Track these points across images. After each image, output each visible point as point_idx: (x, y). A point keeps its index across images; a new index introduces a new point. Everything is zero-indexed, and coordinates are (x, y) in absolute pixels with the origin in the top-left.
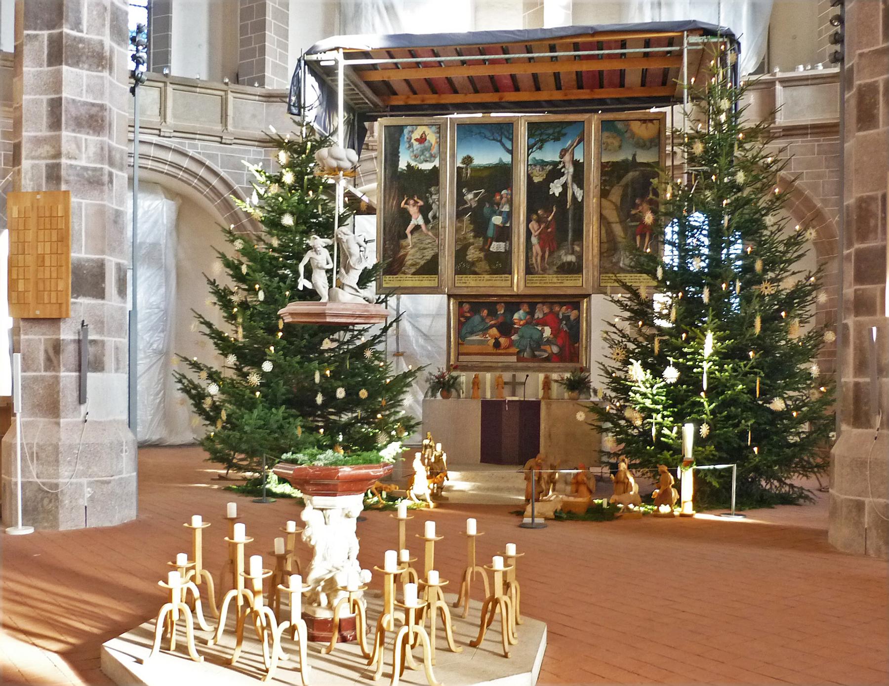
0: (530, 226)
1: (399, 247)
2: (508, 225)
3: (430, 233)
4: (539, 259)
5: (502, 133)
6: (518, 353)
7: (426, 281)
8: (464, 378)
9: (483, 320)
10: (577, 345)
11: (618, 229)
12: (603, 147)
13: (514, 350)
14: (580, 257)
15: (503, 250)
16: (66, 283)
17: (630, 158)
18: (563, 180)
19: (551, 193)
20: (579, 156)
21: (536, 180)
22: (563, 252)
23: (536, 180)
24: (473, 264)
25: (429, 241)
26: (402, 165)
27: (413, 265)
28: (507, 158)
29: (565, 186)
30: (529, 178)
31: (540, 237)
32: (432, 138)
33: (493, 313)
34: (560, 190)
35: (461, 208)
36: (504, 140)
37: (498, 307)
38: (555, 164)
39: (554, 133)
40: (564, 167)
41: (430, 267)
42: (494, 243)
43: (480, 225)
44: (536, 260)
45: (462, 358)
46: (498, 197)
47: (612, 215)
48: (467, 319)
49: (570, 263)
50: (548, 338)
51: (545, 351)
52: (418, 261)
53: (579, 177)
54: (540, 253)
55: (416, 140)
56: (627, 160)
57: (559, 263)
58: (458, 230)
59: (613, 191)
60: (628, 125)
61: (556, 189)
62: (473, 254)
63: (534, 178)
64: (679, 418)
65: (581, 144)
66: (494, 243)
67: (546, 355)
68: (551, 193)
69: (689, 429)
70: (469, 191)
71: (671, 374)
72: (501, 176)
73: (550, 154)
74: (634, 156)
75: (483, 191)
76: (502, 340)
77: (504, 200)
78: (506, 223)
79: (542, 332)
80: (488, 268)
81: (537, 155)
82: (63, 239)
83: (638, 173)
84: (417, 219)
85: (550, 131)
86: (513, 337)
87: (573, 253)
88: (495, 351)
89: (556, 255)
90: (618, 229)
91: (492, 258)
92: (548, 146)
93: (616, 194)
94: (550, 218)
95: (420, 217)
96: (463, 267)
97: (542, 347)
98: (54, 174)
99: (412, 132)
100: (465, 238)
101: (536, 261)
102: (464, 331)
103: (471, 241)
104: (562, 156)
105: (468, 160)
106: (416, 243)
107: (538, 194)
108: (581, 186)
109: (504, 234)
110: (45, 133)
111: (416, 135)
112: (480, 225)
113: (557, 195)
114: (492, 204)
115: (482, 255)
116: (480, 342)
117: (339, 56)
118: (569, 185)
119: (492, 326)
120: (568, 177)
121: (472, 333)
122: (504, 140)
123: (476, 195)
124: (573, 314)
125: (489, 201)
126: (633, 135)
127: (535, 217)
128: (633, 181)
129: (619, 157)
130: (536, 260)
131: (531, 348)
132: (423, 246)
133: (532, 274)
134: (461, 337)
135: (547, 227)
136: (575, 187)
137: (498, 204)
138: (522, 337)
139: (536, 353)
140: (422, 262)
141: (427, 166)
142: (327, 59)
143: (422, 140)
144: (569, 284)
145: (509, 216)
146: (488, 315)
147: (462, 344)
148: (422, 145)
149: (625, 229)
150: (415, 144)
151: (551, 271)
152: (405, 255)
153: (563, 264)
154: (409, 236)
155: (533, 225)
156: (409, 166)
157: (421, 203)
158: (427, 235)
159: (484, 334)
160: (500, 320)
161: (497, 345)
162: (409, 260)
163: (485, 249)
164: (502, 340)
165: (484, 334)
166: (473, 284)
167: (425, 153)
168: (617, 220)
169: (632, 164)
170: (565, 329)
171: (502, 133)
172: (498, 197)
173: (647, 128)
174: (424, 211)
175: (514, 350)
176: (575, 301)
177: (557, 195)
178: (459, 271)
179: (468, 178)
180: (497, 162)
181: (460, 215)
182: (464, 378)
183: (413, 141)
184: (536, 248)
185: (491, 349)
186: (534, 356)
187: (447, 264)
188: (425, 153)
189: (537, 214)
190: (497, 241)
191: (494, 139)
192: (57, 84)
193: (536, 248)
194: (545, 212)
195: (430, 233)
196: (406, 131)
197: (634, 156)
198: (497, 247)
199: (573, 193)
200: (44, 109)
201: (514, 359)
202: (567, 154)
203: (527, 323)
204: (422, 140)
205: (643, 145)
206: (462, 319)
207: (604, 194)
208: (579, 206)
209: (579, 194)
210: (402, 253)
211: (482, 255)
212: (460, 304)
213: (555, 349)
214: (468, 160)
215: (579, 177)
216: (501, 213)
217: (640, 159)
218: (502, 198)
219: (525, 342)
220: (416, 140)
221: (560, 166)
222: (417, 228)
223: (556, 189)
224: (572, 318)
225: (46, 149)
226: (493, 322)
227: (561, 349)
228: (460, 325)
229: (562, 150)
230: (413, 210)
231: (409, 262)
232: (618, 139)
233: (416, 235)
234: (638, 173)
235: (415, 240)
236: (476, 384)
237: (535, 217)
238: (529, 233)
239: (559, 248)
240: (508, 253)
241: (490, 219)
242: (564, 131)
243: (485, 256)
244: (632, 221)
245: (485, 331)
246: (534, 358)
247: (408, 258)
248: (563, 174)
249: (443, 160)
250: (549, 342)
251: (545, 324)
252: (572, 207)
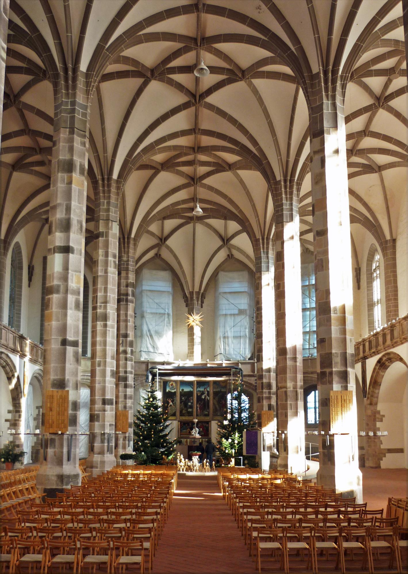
7: (173, 418)
8: (183, 440)
11: (217, 406)
12: (214, 388)
14: (209, 412)
16: (127, 426)
20: (208, 390)
26: (167, 391)
28: (192, 390)
29: (205, 396)
30: (197, 394)
32: (174, 384)
33: (188, 425)
41: (174, 415)
43: (186, 405)
47: (216, 403)
53: (208, 394)
58: (180, 406)
62: (184, 412)
64: (232, 449)
69: (233, 451)
71: (230, 440)
72: (190, 394)
73: (202, 389)
81: (199, 389)
82: (127, 418)
84: (171, 403)
90: (217, 406)
93: (217, 398)
96: (182, 414)
98: (125, 407)
101: (199, 413)
105: (183, 390)
107: (199, 398)
109: (191, 407)
110: (123, 400)
111: (171, 384)
112: (186, 405)
117: (157, 370)
120: (206, 394)
124: (207, 425)
129: (218, 390)
134: (181, 430)
141: (173, 391)
142: (155, 370)
143: (172, 385)
144: (207, 419)
145: (192, 403)
155: (198, 405)
163: (187, 410)
166: (184, 418)
167: (172, 388)
169: (221, 392)
174: (172, 401)
176: (208, 423)
179: (183, 394)
181: (181, 402)
182: (183, 440)
184: (199, 410)
187: (178, 414)
188: (172, 388)
192: (126, 392)
193: (199, 410)
198: (190, 410)
200: (123, 396)
204: (172, 385)
207: (214, 398)
208: (208, 401)
209: (208, 398)
212: (181, 423)
214: (183, 390)
215: (208, 394)
222: (171, 405)
223: (203, 397)
225: (124, 403)
228: (181, 427)
230: (170, 401)
236: (186, 442)
240: (192, 411)
245: (186, 429)
249: (177, 390)
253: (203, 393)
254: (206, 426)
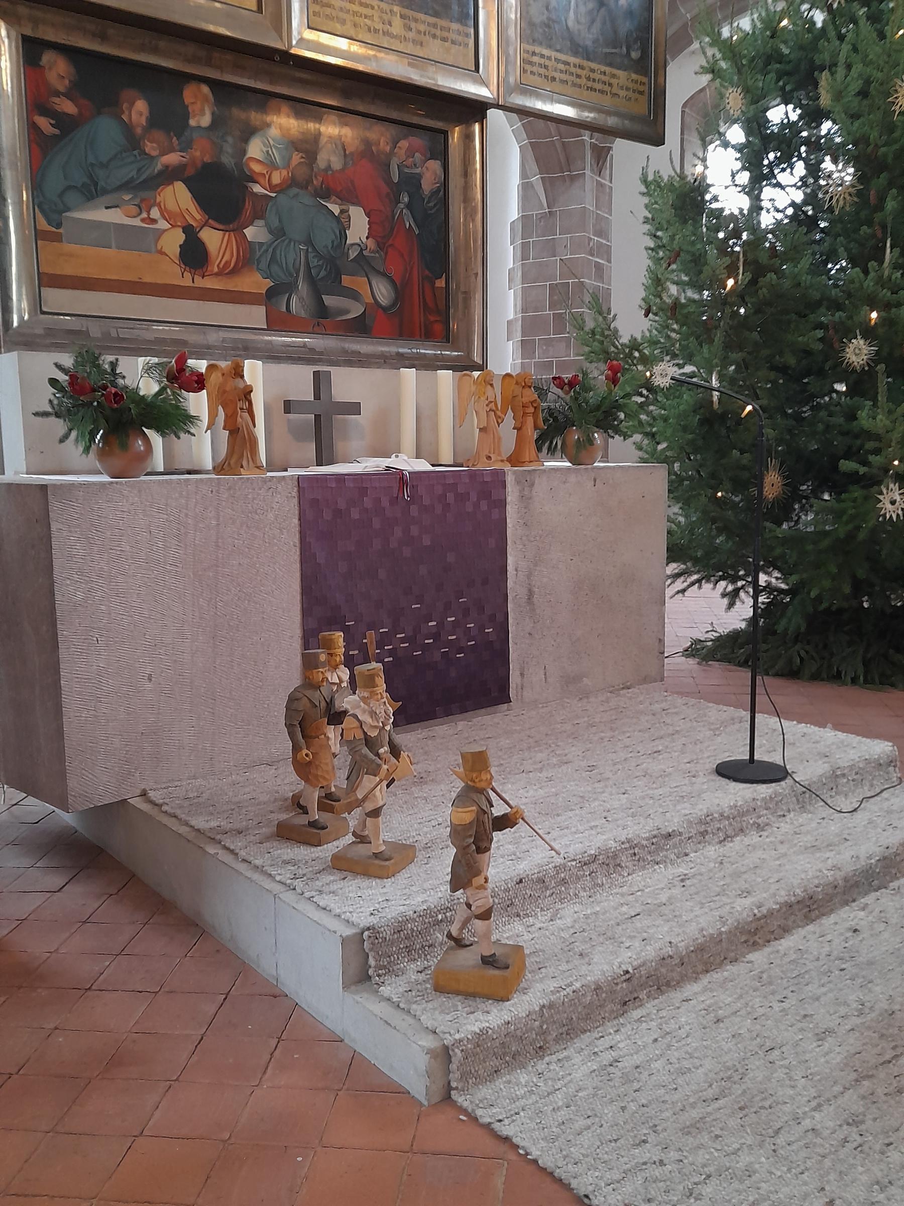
6: (271, 294)
9: (133, 142)
10: (440, 283)
13: (255, 282)
37: (189, 93)
45: (55, 298)
48: (66, 125)
50: (362, 248)
51: (354, 295)
67: (356, 310)
76: (212, 239)
79: (342, 224)
86: (249, 232)
88: (187, 281)
97: (346, 280)
102: (54, 181)
116: (126, 237)
119: (169, 175)
121: (92, 192)
131: (312, 281)
138: (279, 233)
139: (328, 300)
146: (154, 122)
147: (58, 238)
159: (143, 206)
160: (200, 153)
161: (194, 255)
164: (212, 238)
165: (143, 206)
170: (409, 222)
175: (255, 282)
185: (174, 273)
186: (322, 312)
201: (257, 315)
203: (291, 183)
206: (44, 123)
213: (383, 292)
219: (294, 255)
224: (428, 185)
226: (173, 158)
227: (400, 292)
246: (322, 318)
250: (363, 264)
251: (349, 197)
254: (412, 182)
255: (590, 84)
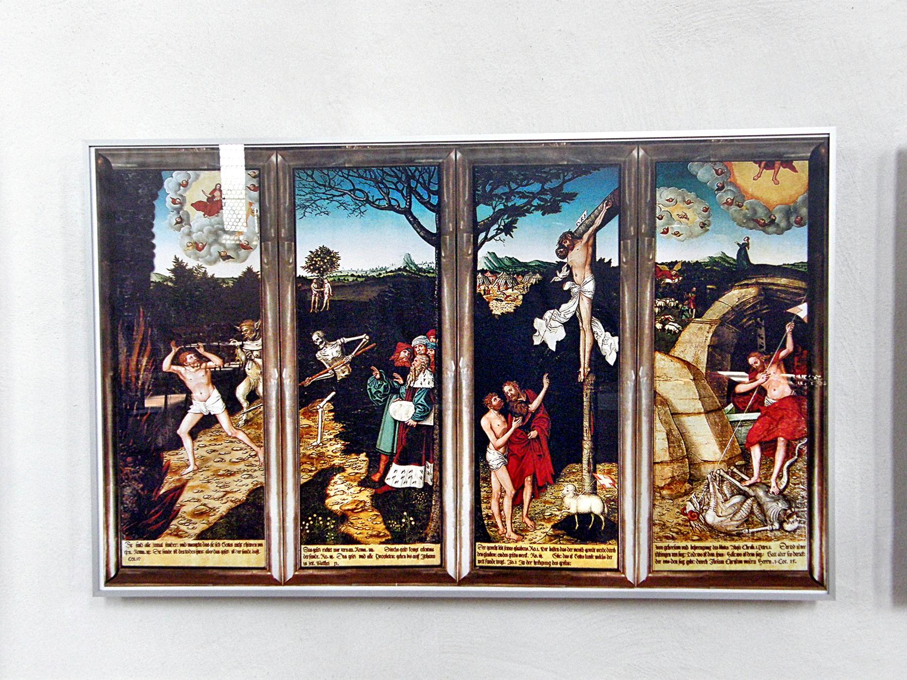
0: (484, 422)
1: (159, 470)
2: (430, 422)
3: (241, 436)
4: (507, 503)
5: (412, 191)
15: (419, 485)
17: (733, 254)
18: (568, 309)
19: (537, 341)
21: (498, 309)
22: (568, 489)
23: (498, 309)
24: (343, 518)
25: (240, 454)
26: (163, 267)
27: (200, 514)
29: (572, 326)
31: (511, 450)
34: (561, 334)
35: (308, 382)
36: (418, 209)
38: (547, 270)
39: (543, 191)
40: (570, 277)
42: (394, 466)
44: (500, 505)
46: (404, 354)
49: (585, 517)
52: (212, 504)
54: (510, 490)
55: (198, 206)
56: (724, 258)
57: (559, 516)
59: (685, 336)
60: (725, 174)
61: (549, 331)
62: (342, 494)
63: (493, 305)
65: (614, 223)
66: (394, 466)
68: (537, 341)
70: (330, 338)
73: (532, 242)
74: (743, 249)
75: (365, 338)
77: (420, 360)
78: (426, 417)
80: (381, 527)
83: (753, 291)
84: (207, 401)
85: (535, 187)
87: (594, 491)
89: (548, 497)
91: (389, 502)
92: (522, 222)
94: (533, 406)
95: (216, 393)
99: (185, 185)
100: (321, 456)
103: (337, 462)
104: (564, 250)
106: (204, 460)
108: (613, 327)
109: (419, 444)
113: (552, 347)
114: (390, 369)
115: (365, 495)
118: (585, 324)
122: (418, 209)
123: (346, 349)
125: (381, 361)
126: (739, 198)
127: (495, 401)
128: (738, 311)
130: (500, 505)
132: (224, 467)
133: (488, 539)
135: (526, 428)
136: (599, 328)
137: (404, 372)
140: (223, 508)
148: (214, 219)
149: (723, 432)
150: (198, 219)
151: (539, 535)
152: (179, 490)
153: (570, 517)
154: (187, 442)
155: (492, 421)
156: (179, 269)
157: (215, 361)
158: (234, 439)
162: (188, 502)
168: (699, 406)
171: (412, 191)
172: (404, 354)
173: (776, 182)
177: (552, 347)
178: (311, 536)
180: (400, 264)
183: (188, 207)
187: (282, 510)
189: (502, 395)
190: (401, 463)
191: (391, 208)
193: (501, 478)
194: (523, 387)
195: (241, 436)
196: (171, 182)
197: (743, 249)
199: (595, 343)
202: (579, 246)
205: (766, 222)
210: (169, 483)
211: (365, 495)
214: (324, 259)
216: (411, 394)
217: (756, 258)
218: (413, 355)
220: (198, 206)
221: (560, 276)
222: (208, 422)
223: (549, 331)
229: (564, 237)
231: (189, 508)
232: (699, 207)
233: (204, 438)
234: (753, 291)
235: (202, 452)
237: (495, 401)
238: (481, 442)
239: (556, 478)
240: (433, 491)
241: (382, 409)
242: (568, 188)
243: (373, 497)
244: (738, 410)
247: (186, 495)
248: (567, 296)
252: (592, 379)
253: (546, 291)
255: (733, 558)
